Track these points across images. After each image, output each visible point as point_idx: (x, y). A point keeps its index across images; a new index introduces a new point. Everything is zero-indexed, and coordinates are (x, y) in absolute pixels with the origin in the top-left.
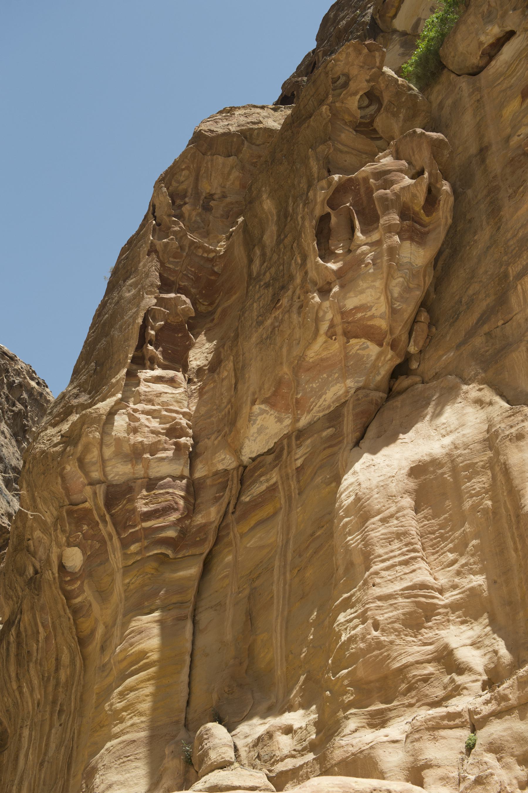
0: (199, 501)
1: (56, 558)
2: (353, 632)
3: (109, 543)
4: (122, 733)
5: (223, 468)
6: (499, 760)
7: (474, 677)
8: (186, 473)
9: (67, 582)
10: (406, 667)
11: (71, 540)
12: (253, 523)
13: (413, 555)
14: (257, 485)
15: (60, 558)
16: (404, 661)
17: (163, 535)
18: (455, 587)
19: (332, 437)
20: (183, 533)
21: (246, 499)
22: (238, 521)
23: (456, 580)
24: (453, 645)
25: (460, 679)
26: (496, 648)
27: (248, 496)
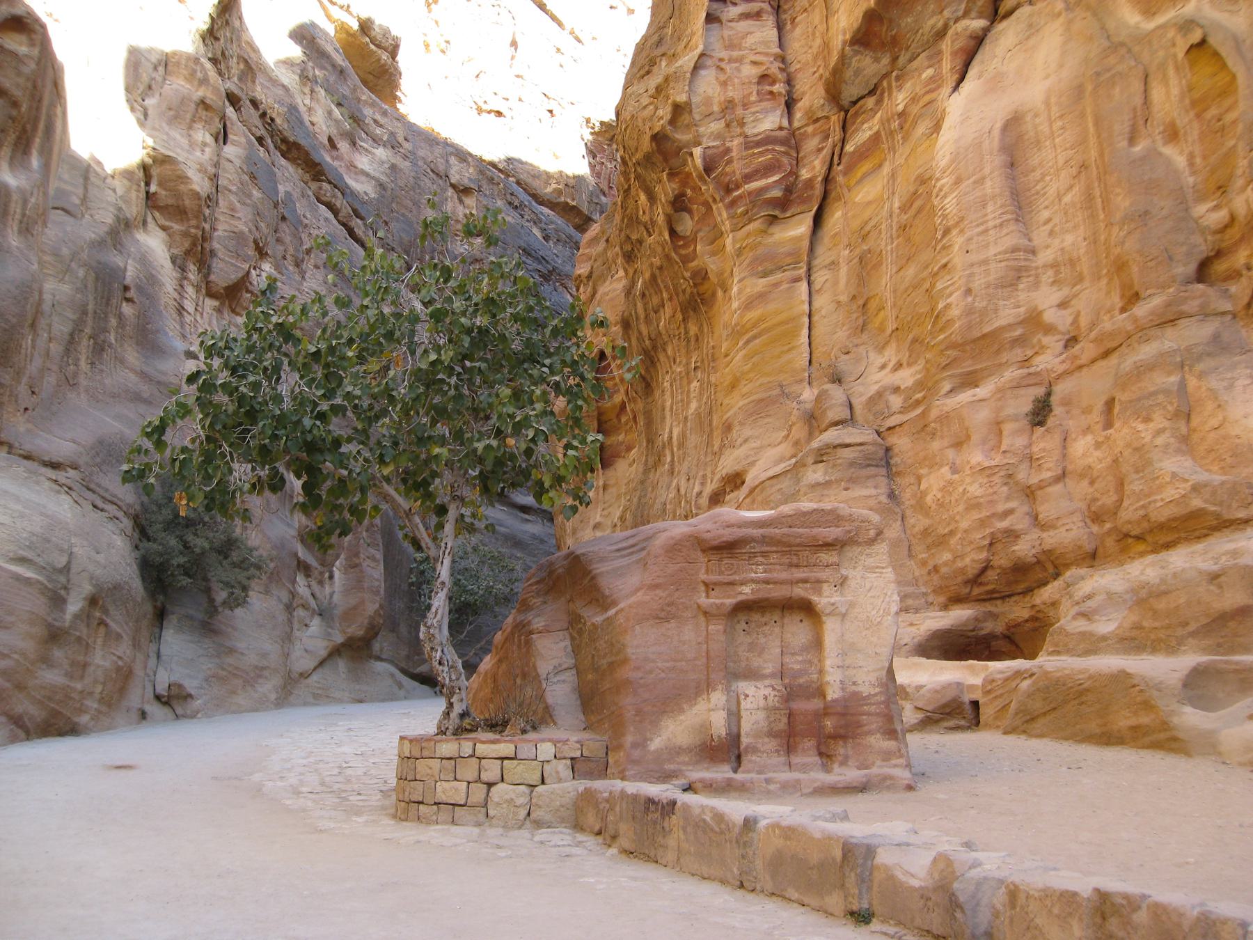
8: (785, 123)
9: (681, 247)
10: (1001, 329)
12: (859, 174)
16: (995, 325)
19: (932, 79)
20: (788, 190)
21: (849, 148)
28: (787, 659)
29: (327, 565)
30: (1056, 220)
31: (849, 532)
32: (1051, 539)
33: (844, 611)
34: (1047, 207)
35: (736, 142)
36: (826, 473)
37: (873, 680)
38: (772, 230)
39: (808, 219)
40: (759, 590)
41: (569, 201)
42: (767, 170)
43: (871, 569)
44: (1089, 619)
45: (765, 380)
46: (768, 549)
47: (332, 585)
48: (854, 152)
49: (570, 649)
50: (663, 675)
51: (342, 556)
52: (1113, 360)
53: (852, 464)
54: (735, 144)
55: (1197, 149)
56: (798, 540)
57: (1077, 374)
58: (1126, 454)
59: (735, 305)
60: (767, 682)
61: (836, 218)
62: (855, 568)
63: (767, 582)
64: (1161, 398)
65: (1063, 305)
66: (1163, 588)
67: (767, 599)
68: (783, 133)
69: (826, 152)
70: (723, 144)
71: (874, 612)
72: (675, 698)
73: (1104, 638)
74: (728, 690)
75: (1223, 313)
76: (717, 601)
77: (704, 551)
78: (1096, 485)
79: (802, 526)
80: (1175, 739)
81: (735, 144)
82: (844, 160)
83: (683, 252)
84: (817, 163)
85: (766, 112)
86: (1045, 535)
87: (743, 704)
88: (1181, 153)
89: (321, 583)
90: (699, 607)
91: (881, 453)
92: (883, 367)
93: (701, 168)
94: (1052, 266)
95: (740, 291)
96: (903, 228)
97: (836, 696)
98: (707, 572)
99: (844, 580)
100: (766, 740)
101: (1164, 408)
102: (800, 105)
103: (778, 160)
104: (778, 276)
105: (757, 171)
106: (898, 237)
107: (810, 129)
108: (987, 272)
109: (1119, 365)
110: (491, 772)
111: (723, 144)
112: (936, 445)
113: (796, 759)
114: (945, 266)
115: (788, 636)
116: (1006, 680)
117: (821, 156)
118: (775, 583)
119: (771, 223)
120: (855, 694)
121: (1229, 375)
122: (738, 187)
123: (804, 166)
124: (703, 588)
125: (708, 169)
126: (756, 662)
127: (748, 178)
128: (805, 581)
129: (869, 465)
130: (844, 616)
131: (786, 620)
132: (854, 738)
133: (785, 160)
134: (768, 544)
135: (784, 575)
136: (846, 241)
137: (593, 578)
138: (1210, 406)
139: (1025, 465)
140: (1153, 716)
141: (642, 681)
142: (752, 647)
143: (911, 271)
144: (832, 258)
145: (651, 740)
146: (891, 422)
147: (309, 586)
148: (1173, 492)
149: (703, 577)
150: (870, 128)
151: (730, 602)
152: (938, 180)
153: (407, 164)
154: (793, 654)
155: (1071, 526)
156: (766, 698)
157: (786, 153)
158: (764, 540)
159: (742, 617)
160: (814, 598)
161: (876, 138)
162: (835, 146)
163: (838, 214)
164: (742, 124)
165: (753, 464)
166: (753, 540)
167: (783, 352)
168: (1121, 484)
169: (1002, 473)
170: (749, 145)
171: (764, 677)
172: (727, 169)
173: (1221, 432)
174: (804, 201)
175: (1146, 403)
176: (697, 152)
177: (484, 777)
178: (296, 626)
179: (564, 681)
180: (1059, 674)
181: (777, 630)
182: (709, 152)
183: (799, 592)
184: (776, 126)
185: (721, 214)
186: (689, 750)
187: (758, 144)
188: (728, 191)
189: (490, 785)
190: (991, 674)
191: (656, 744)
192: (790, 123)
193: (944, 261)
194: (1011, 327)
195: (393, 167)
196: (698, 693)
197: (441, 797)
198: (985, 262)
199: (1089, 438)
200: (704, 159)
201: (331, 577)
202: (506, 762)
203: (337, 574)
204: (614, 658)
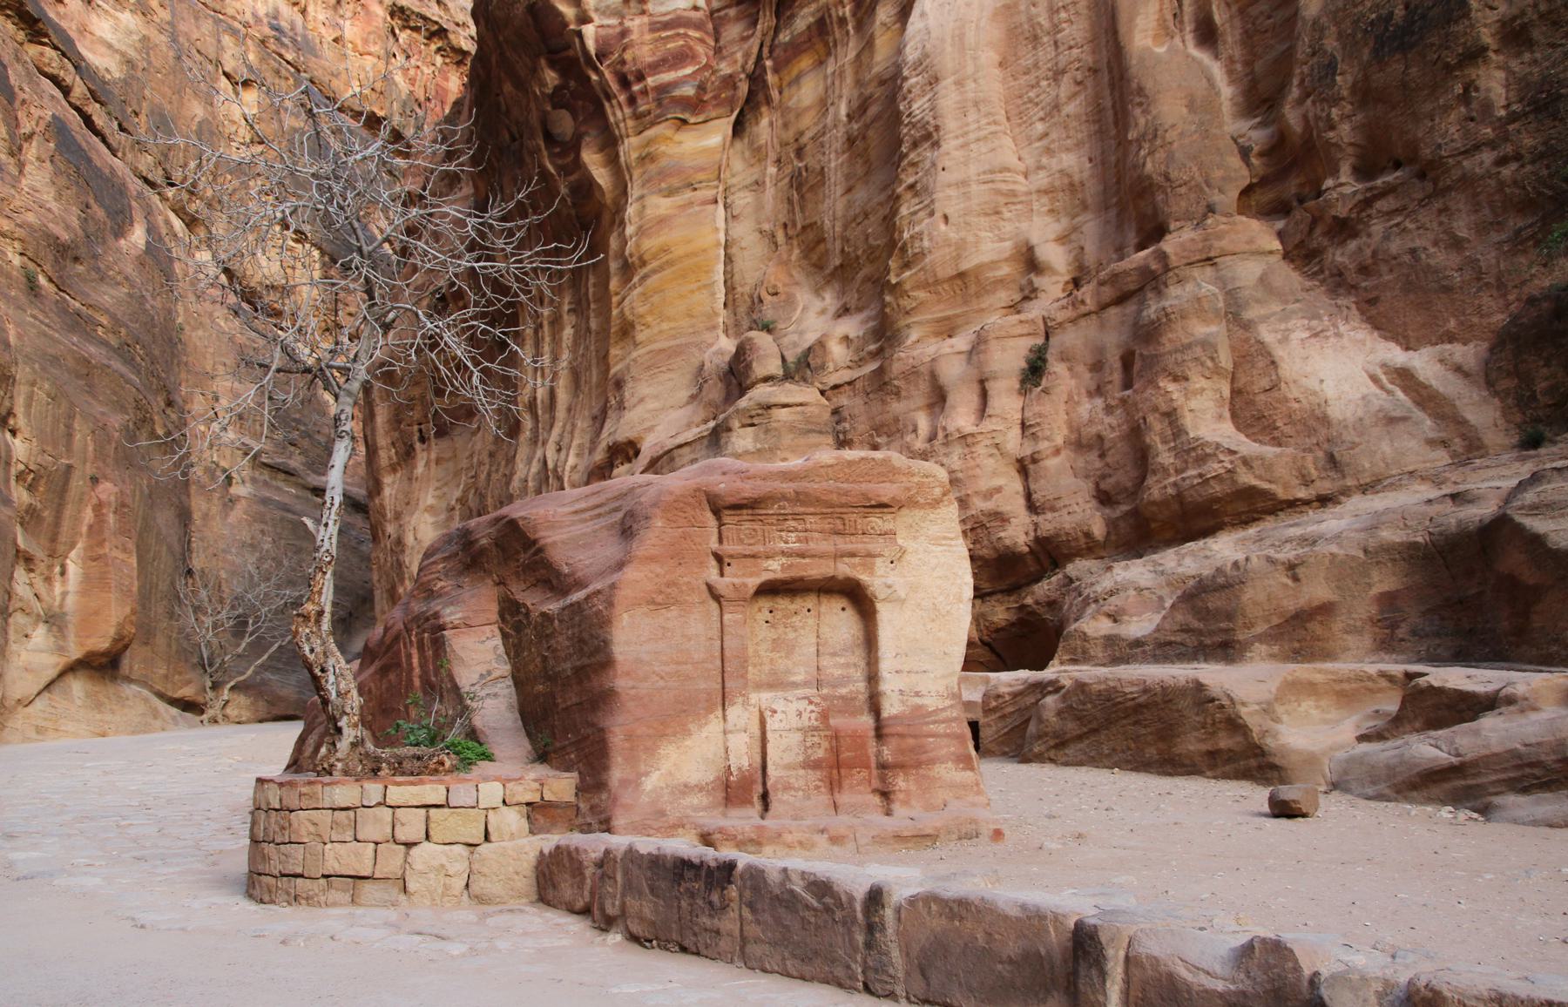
0: (722, 43)
2: (917, 229)
3: (607, 105)
4: (650, 341)
6: (1070, 369)
7: (1054, 279)
10: (980, 268)
12: (795, 72)
13: (993, 128)
15: (544, 123)
17: (677, 93)
18: (1040, 168)
20: (701, 88)
21: (784, 37)
23: (1044, 160)
24: (1034, 241)
25: (1038, 281)
26: (1082, 243)
28: (826, 662)
29: (56, 554)
30: (1054, 135)
31: (908, 489)
32: (1049, 524)
33: (903, 596)
34: (1042, 119)
36: (756, 439)
37: (942, 689)
38: (679, 137)
39: (725, 125)
40: (791, 566)
41: (376, 110)
43: (936, 541)
44: (1115, 621)
45: (665, 326)
46: (802, 510)
47: (64, 583)
49: (501, 649)
50: (661, 683)
51: (80, 545)
52: (1131, 308)
53: (792, 428)
54: (636, 24)
55: (1237, 52)
56: (844, 500)
57: (1083, 322)
58: (1150, 419)
59: (630, 230)
60: (800, 692)
61: (764, 127)
62: (915, 538)
63: (802, 555)
64: (1198, 351)
65: (1062, 239)
66: (1221, 580)
67: (801, 579)
68: (699, 15)
69: (754, 44)
70: (621, 24)
71: (941, 598)
72: (677, 716)
73: (1138, 643)
74: (746, 704)
75: (1271, 252)
76: (736, 581)
77: (717, 512)
78: (1109, 459)
79: (847, 481)
80: (1274, 767)
82: (778, 52)
83: (560, 162)
86: (1040, 519)
87: (771, 724)
88: (1217, 57)
89: (48, 580)
90: (710, 588)
91: (827, 416)
92: (823, 312)
93: (593, 52)
94: (1046, 192)
95: (641, 213)
96: (851, 141)
97: (894, 711)
98: (720, 541)
99: (903, 551)
100: (802, 772)
101: (1202, 364)
103: (691, 48)
104: (688, 195)
105: (664, 60)
107: (732, 12)
108: (967, 196)
109: (1140, 311)
110: (412, 824)
111: (621, 24)
112: (897, 407)
113: (844, 798)
114: (912, 187)
115: (825, 630)
116: (1015, 695)
118: (813, 556)
120: (919, 707)
121: (1283, 326)
123: (723, 58)
124: (714, 562)
125: (601, 55)
126: (782, 664)
127: (656, 67)
128: (853, 555)
129: (810, 431)
130: (903, 601)
131: (823, 609)
132: (918, 765)
133: (700, 49)
134: (803, 503)
135: (826, 546)
136: (772, 156)
137: (540, 550)
138: (1261, 363)
139: (1017, 430)
140: (1239, 739)
141: (633, 692)
142: (776, 644)
143: (861, 194)
144: (755, 177)
145: (647, 774)
146: (833, 379)
147: (31, 585)
148: (1216, 466)
149: (714, 545)
150: (813, 14)
151: (753, 582)
152: (906, 79)
153: (163, 38)
154: (834, 654)
155: (1076, 508)
156: (800, 714)
157: (702, 41)
158: (800, 498)
159: (765, 603)
160: (864, 577)
163: (765, 122)
165: (651, 429)
166: (784, 497)
167: (692, 292)
168: (1142, 457)
169: (988, 442)
171: (795, 685)
173: (1275, 394)
175: (1179, 356)
176: (589, 31)
177: (402, 835)
178: (12, 636)
179: (495, 695)
180: (1103, 687)
181: (811, 621)
182: (602, 32)
183: (844, 569)
185: (618, 114)
186: (700, 788)
189: (409, 845)
190: (996, 687)
191: (651, 782)
193: (911, 180)
194: (994, 264)
195: (145, 39)
196: (710, 710)
197: (332, 866)
198: (964, 183)
199: (1099, 402)
200: (597, 41)
201: (63, 573)
202: (433, 811)
203: (72, 568)
204: (586, 661)
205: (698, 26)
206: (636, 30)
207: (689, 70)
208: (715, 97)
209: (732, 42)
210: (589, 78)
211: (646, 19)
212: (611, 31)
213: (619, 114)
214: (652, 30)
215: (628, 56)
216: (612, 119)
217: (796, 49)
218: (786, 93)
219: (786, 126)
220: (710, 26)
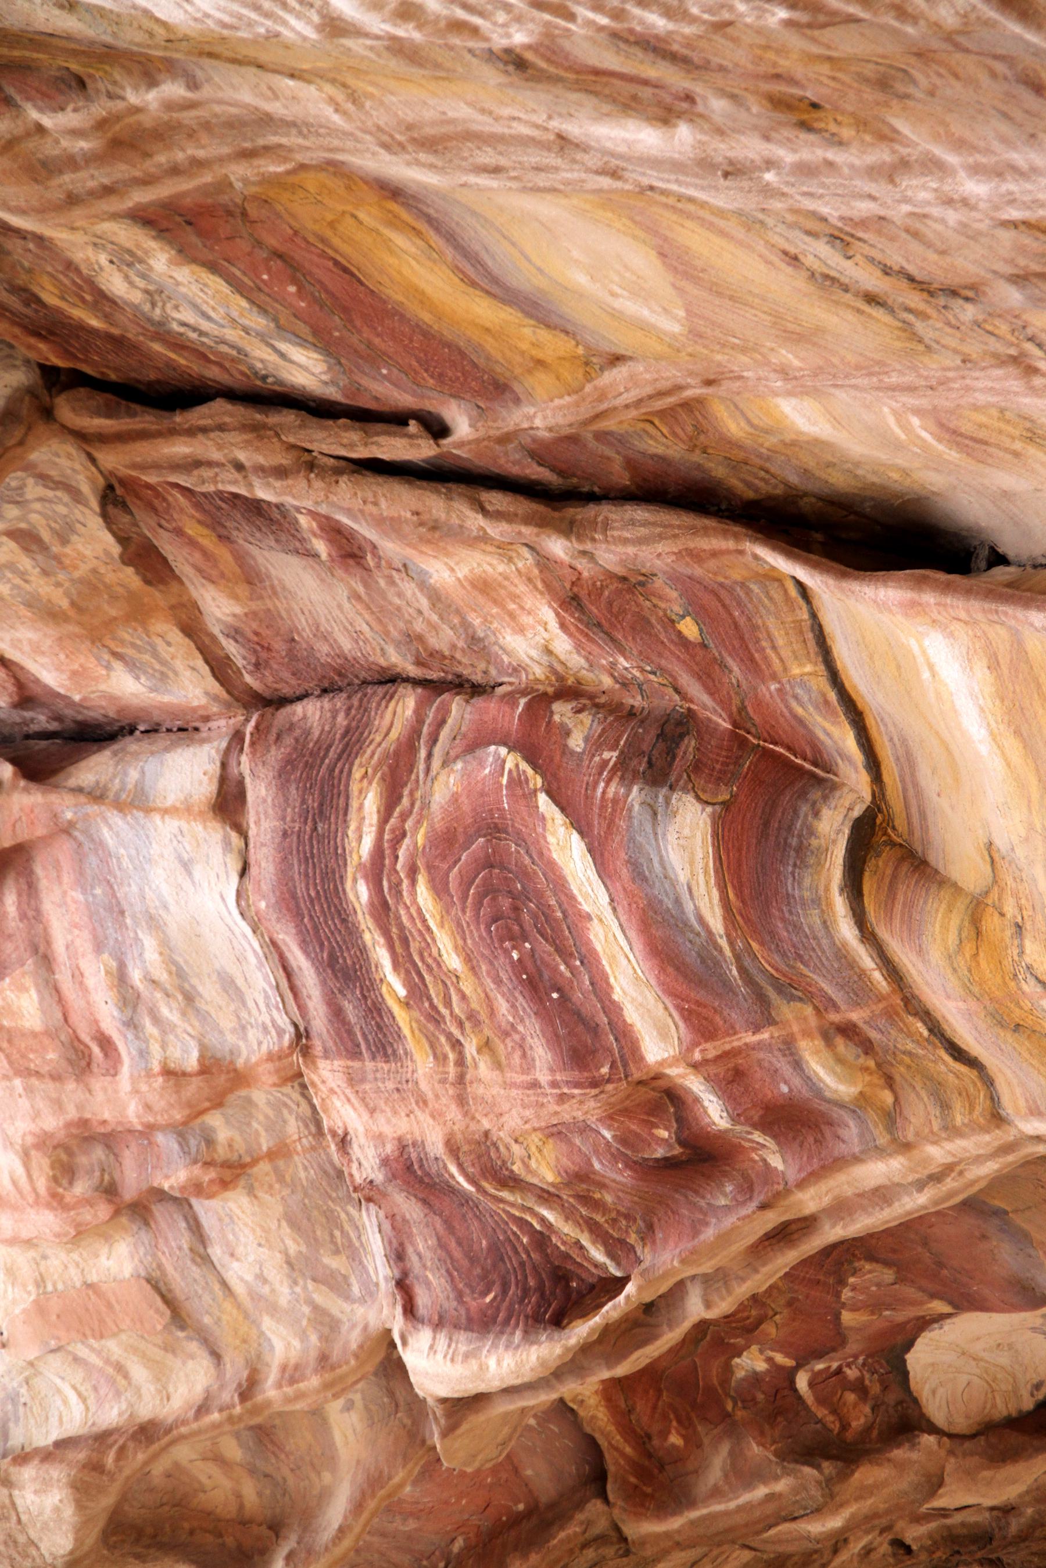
1: (1010, 1470)
3: (833, 1233)
5: (95, 523)
8: (185, 772)
11: (860, 1417)
12: (484, 311)
14: (188, 316)
17: (706, 905)
20: (660, 749)
21: (305, 369)
22: (494, 389)
27: (282, 355)
35: (345, 1113)
38: (965, 866)
39: (877, 620)
42: (515, 909)
48: (321, 340)
54: (365, 1119)
70: (370, 1194)
81: (365, 1119)
82: (387, 390)
84: (446, 570)
85: (111, 914)
102: (49, 674)
103: (447, 842)
105: (535, 983)
106: (887, 136)
107: (219, 607)
111: (370, 1194)
117: (390, 547)
119: (917, 864)
122: (671, 1100)
123: (477, 644)
125: (556, 1293)
127: (587, 1038)
133: (445, 786)
150: (128, 260)
161: (193, 225)
162: (308, 463)
164: (219, 1079)
170: (369, 1038)
172: (545, 1170)
174: (729, 627)
176: (436, 1366)
182: (433, 1289)
184: (212, 840)
185: (880, 1183)
187: (346, 970)
188: (701, 1159)
192: (184, 729)
200: (484, 1324)
205: (318, 785)
206: (396, 1125)
207: (569, 852)
208: (708, 674)
209: (381, 612)
210: (702, 1327)
211: (328, 1074)
212: (422, 1245)
213: (876, 1171)
214: (384, 1044)
215: (545, 1170)
216: (915, 1202)
217: (340, 301)
218: (621, 341)
219: (799, 337)
220: (311, 713)
